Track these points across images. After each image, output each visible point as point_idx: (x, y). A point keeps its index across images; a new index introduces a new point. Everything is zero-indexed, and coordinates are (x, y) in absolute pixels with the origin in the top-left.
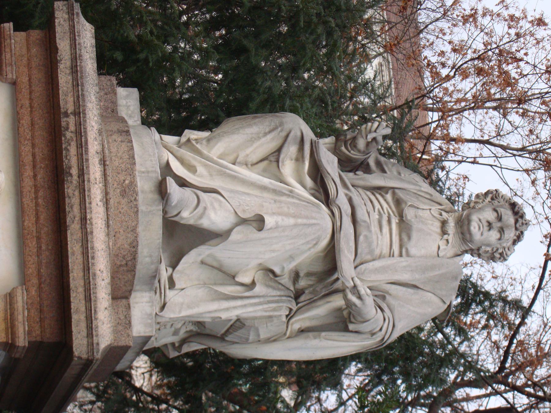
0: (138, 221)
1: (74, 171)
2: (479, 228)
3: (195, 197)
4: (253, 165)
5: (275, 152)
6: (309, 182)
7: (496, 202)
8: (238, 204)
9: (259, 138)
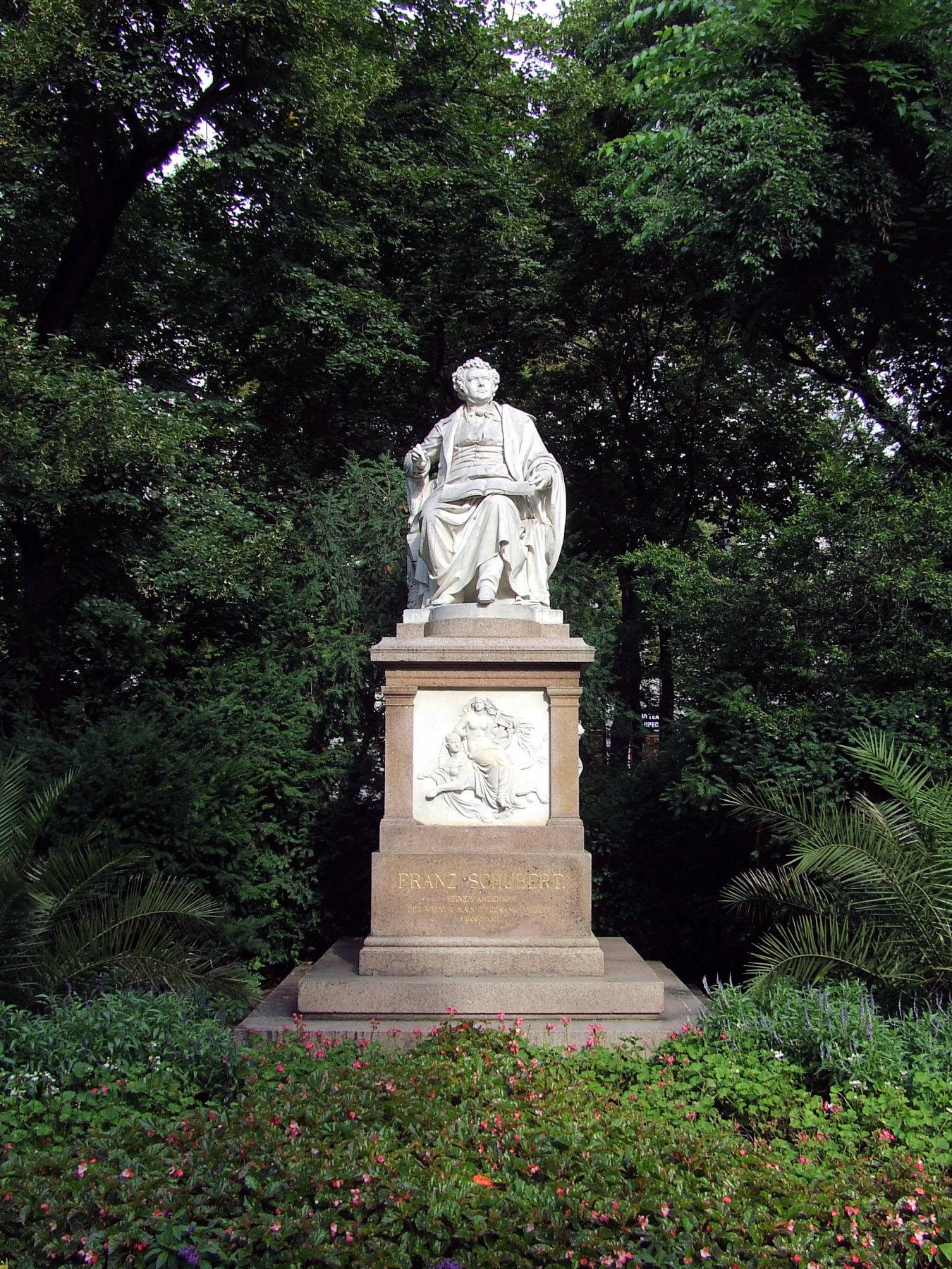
1: (480, 655)
6: (467, 506)
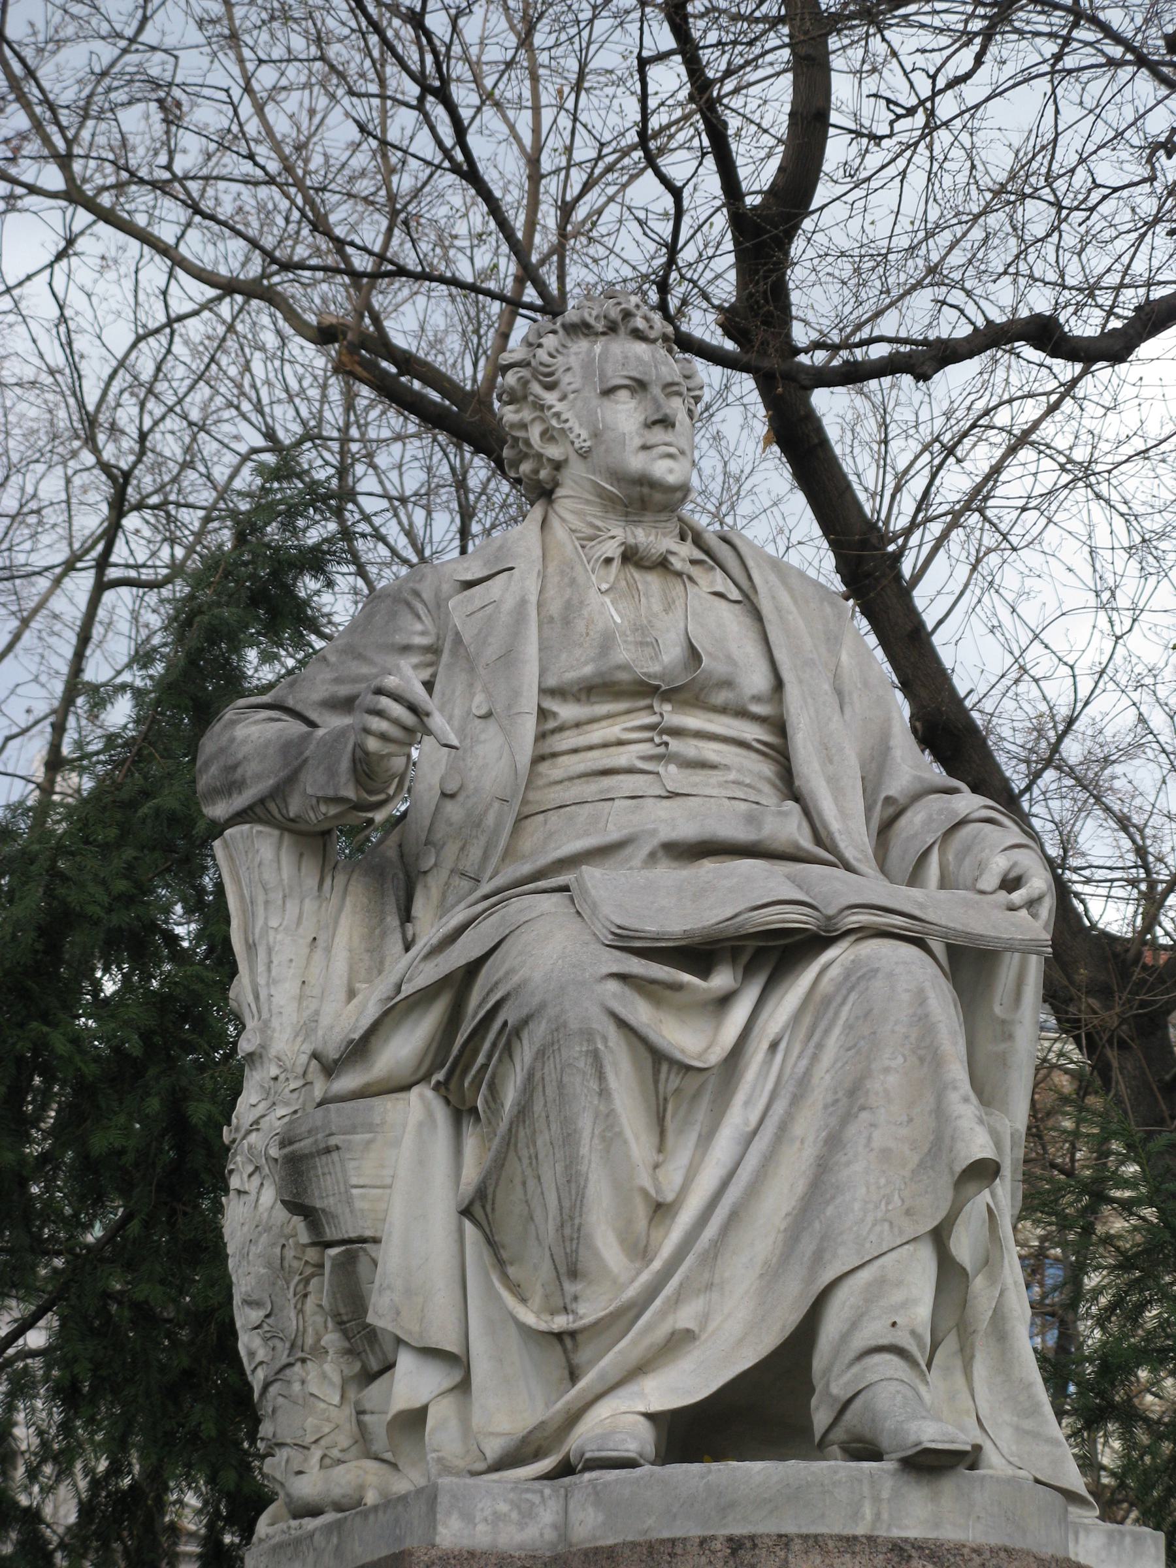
0: (1028, 1554)
2: (670, 456)
3: (877, 1358)
4: (661, 1149)
5: (656, 1072)
6: (722, 979)
7: (567, 379)
8: (886, 1226)
9: (611, 1114)
